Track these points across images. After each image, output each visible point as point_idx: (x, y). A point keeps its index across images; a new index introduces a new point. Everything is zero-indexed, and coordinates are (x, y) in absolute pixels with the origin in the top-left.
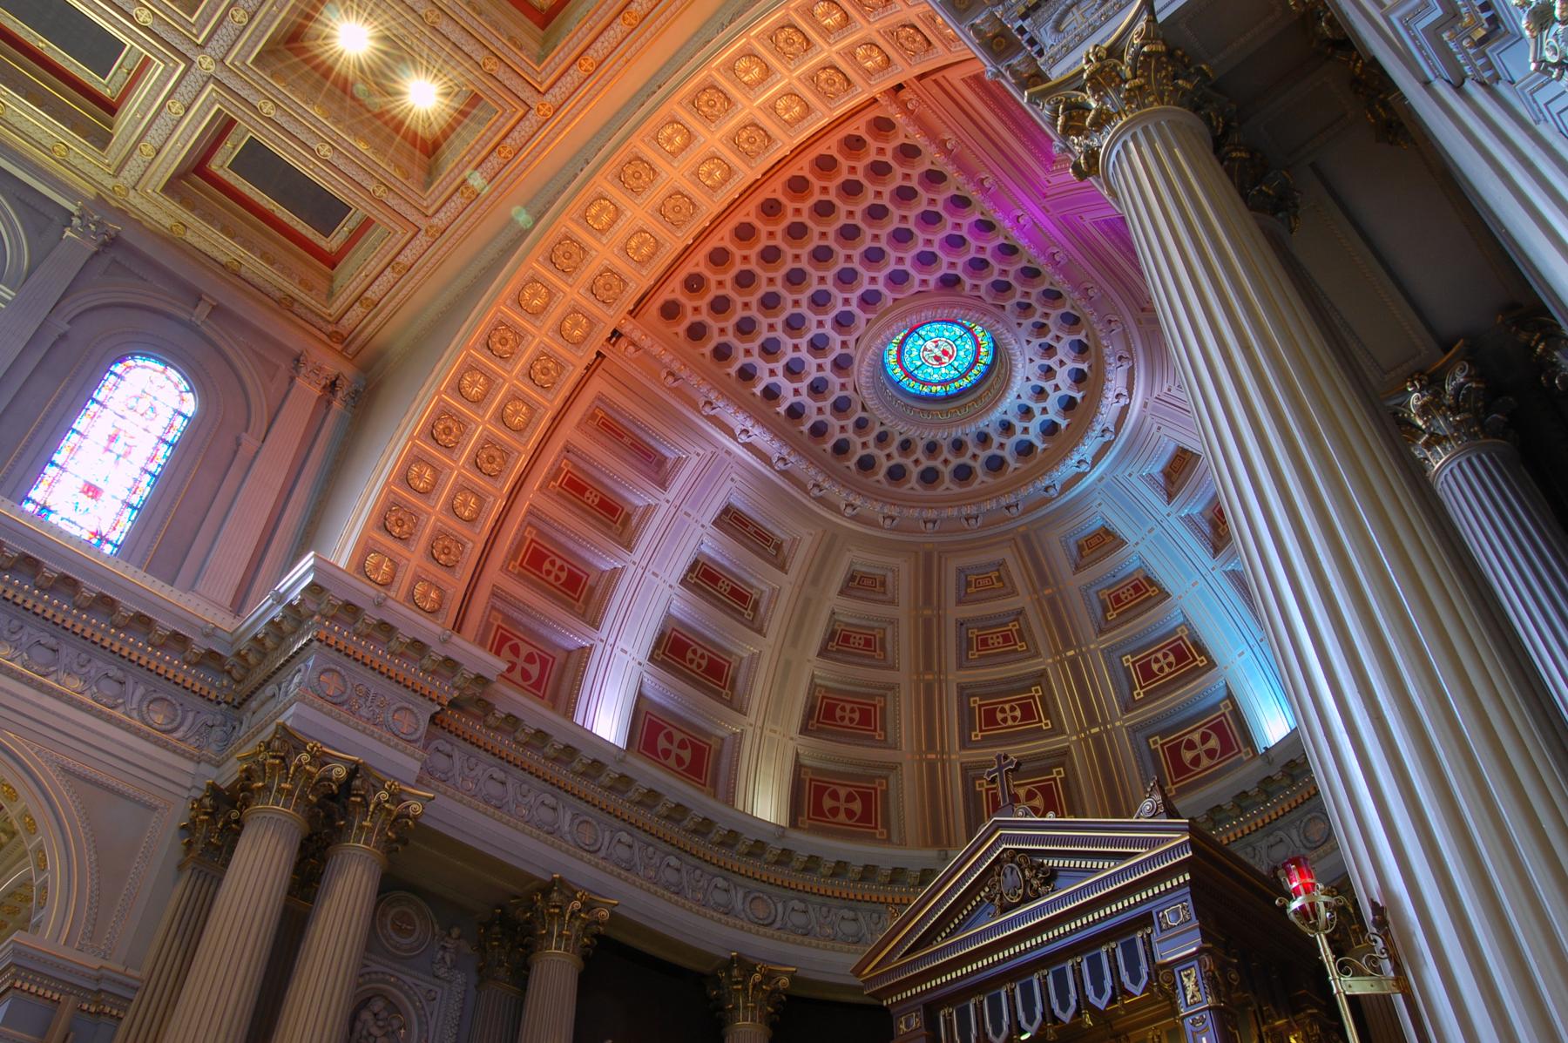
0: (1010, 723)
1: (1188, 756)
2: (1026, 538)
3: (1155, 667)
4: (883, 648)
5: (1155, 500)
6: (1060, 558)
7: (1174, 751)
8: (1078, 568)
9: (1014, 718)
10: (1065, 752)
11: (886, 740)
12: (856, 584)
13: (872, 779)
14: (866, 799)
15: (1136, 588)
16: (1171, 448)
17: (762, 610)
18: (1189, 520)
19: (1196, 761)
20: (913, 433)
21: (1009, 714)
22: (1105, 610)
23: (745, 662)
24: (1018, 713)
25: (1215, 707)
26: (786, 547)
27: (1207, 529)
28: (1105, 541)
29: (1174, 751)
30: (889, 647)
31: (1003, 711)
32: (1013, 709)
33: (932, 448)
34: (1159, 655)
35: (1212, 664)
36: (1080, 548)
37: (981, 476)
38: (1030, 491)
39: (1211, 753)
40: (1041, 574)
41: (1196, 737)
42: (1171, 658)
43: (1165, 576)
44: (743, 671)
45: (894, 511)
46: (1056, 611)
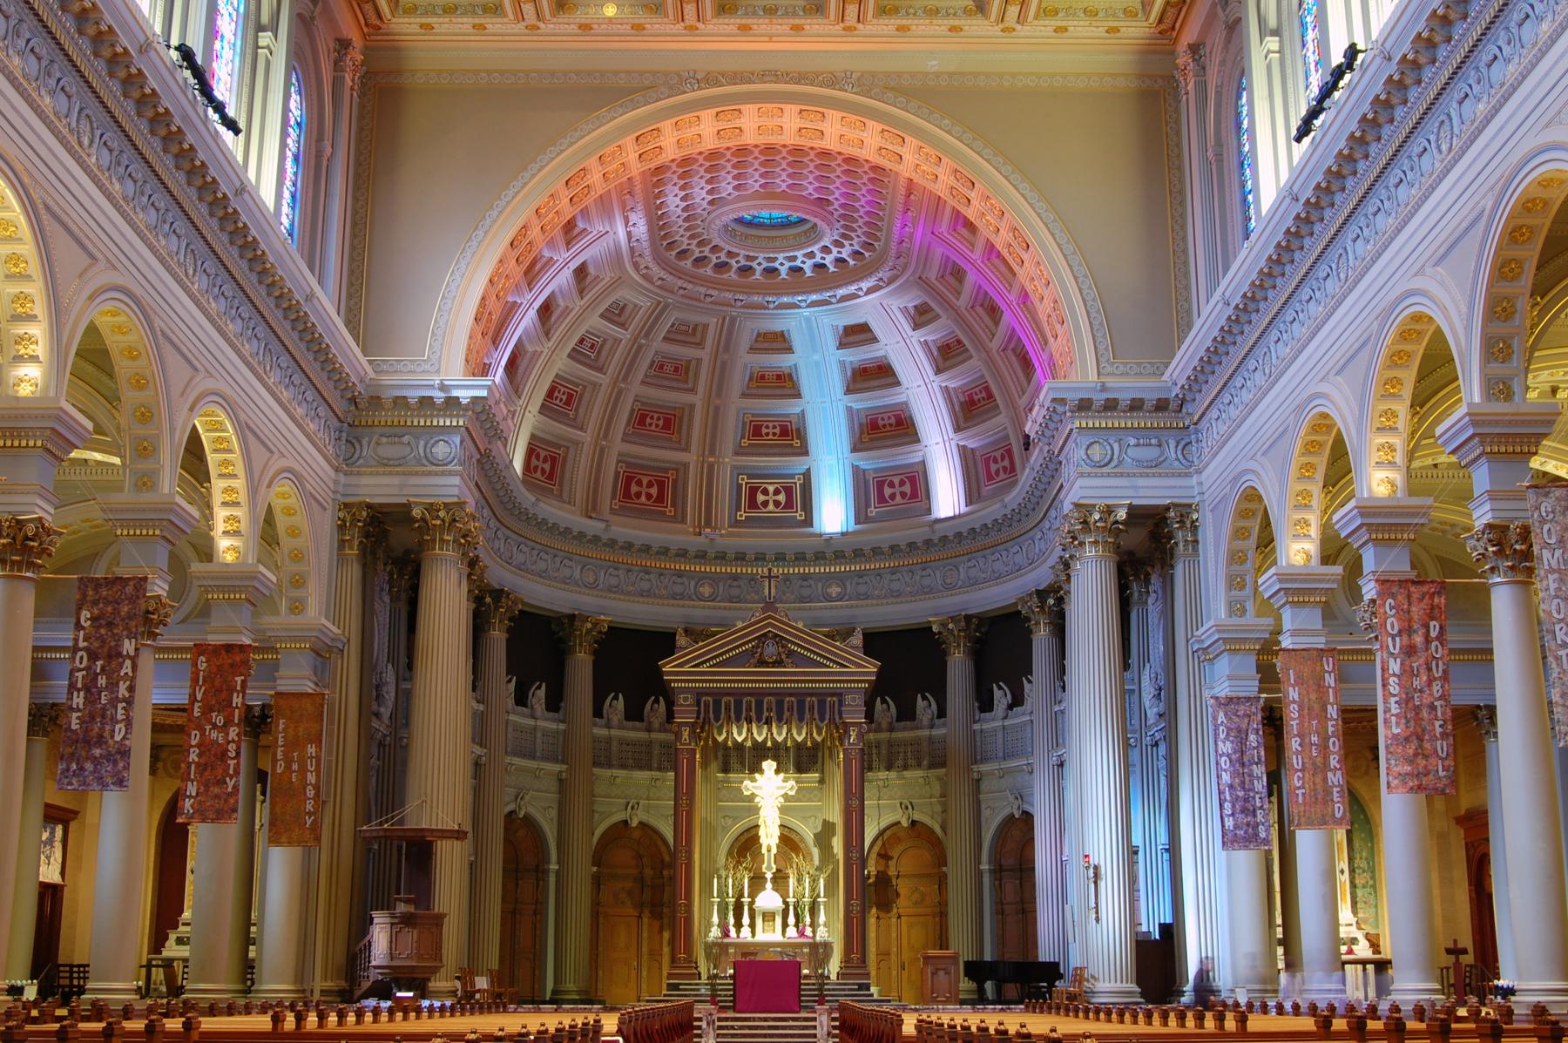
0: (653, 428)
1: (761, 498)
2: (733, 320)
3: (764, 431)
4: (599, 352)
5: (831, 342)
6: (745, 340)
7: (753, 491)
8: (752, 350)
9: (657, 426)
10: (686, 466)
11: (575, 419)
12: (616, 314)
13: (559, 446)
14: (554, 460)
15: (779, 377)
16: (862, 321)
17: (553, 319)
18: (842, 364)
19: (765, 504)
20: (722, 244)
21: (655, 422)
22: (751, 379)
23: (528, 355)
24: (661, 423)
25: (792, 476)
26: (589, 279)
27: (849, 374)
28: (779, 342)
29: (753, 491)
30: (604, 354)
31: (652, 418)
32: (659, 419)
33: (715, 249)
34: (771, 425)
35: (806, 453)
36: (759, 335)
37: (732, 275)
38: (756, 299)
39: (777, 504)
40: (727, 342)
41: (771, 489)
42: (777, 431)
43: (806, 383)
44: (525, 361)
45: (669, 278)
46: (721, 371)
